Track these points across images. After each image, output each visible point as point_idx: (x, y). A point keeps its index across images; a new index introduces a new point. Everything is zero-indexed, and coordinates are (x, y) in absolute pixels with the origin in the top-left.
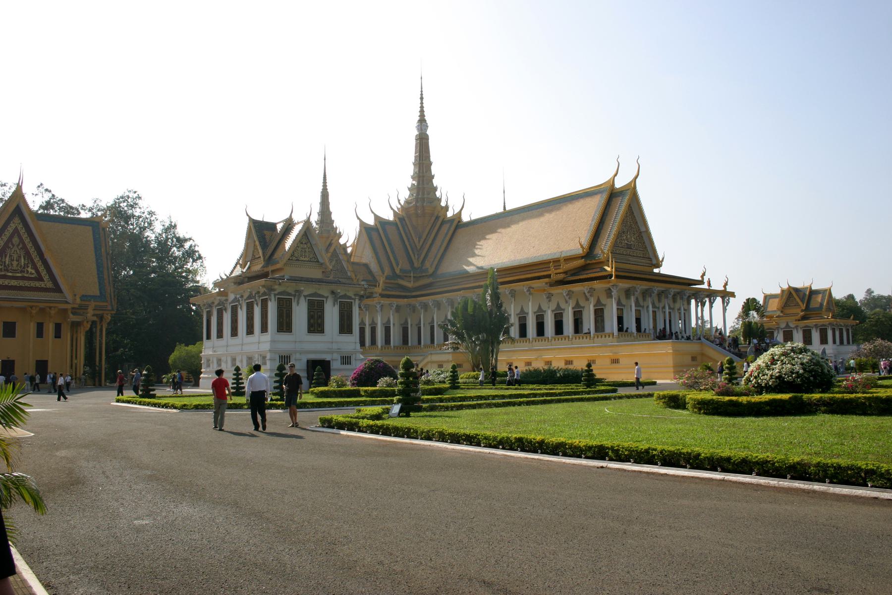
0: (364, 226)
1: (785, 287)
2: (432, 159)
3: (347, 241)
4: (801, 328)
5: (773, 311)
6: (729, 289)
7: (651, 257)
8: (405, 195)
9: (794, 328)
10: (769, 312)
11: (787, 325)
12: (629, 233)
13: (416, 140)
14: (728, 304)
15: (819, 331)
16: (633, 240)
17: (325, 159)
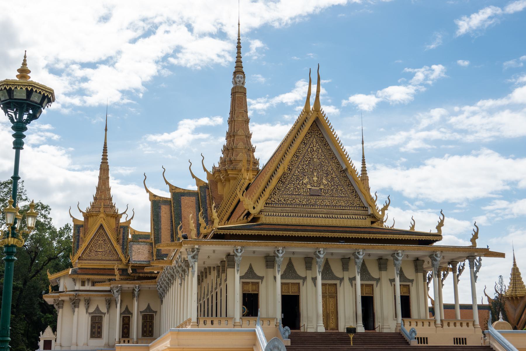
3: (132, 218)
6: (480, 244)
12: (315, 174)
14: (478, 268)
16: (325, 182)
17: (106, 130)
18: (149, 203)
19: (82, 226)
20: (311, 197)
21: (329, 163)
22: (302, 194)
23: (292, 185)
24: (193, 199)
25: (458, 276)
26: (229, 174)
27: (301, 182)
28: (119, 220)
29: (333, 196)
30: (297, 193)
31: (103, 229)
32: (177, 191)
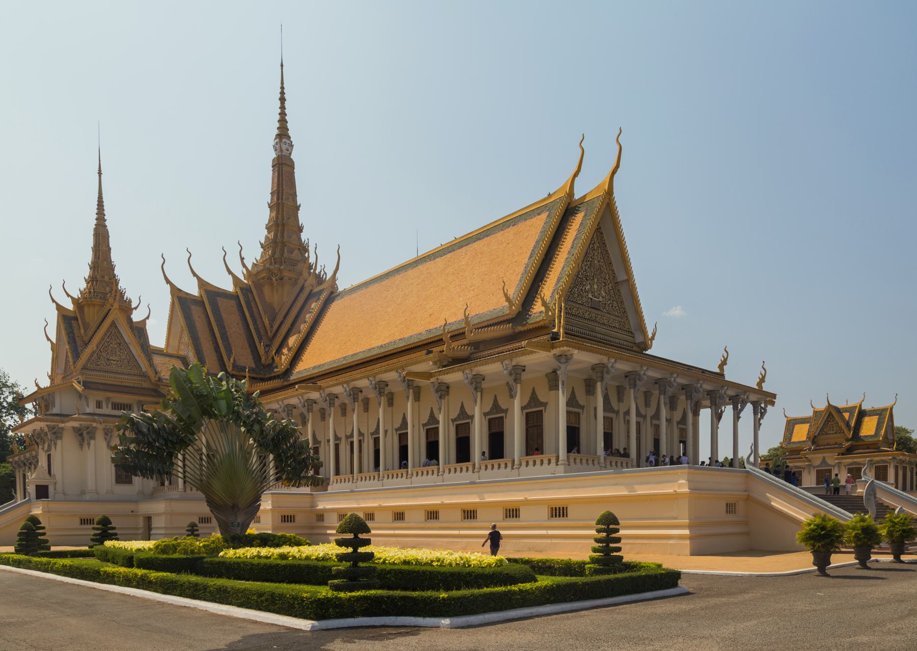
0: (180, 299)
1: (822, 406)
2: (300, 200)
3: (148, 318)
4: (845, 466)
5: (800, 442)
6: (766, 387)
7: (633, 331)
8: (254, 254)
9: (834, 466)
10: (794, 443)
11: (824, 461)
12: (596, 280)
13: (273, 167)
15: (873, 470)
16: (604, 294)
18: (168, 299)
19: (76, 319)
20: (593, 310)
21: (606, 269)
22: (584, 304)
23: (576, 289)
24: (233, 303)
25: (760, 420)
26: (285, 276)
27: (584, 289)
28: (131, 320)
29: (609, 313)
30: (580, 302)
31: (116, 327)
32: (209, 289)
